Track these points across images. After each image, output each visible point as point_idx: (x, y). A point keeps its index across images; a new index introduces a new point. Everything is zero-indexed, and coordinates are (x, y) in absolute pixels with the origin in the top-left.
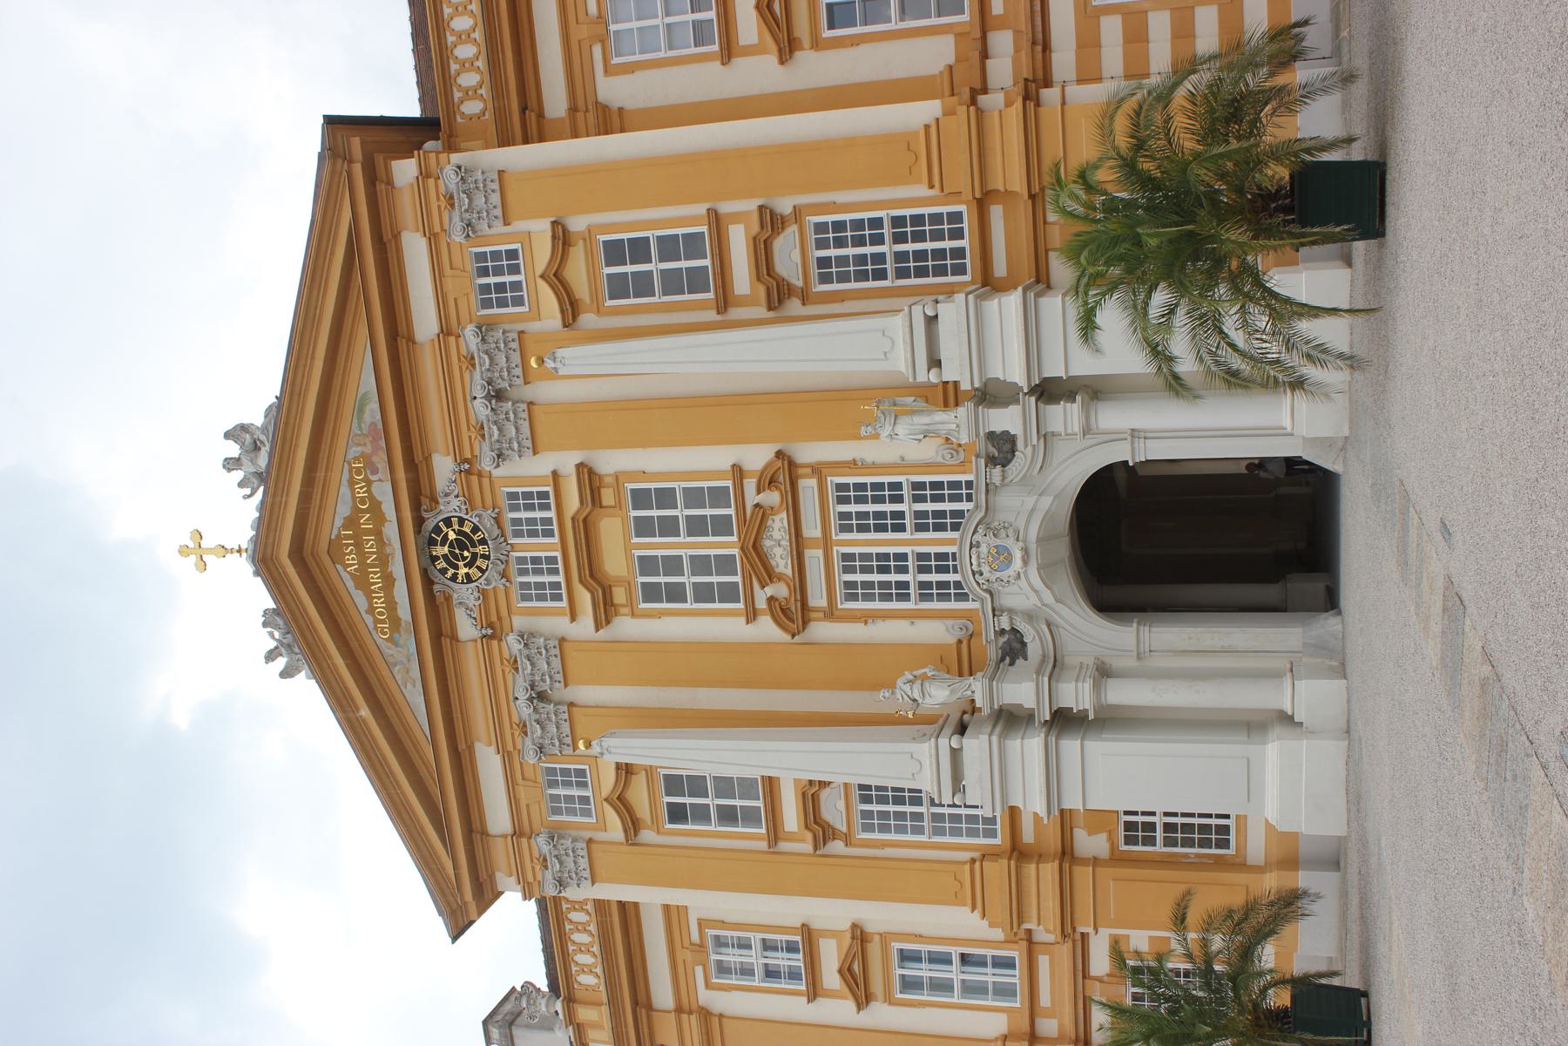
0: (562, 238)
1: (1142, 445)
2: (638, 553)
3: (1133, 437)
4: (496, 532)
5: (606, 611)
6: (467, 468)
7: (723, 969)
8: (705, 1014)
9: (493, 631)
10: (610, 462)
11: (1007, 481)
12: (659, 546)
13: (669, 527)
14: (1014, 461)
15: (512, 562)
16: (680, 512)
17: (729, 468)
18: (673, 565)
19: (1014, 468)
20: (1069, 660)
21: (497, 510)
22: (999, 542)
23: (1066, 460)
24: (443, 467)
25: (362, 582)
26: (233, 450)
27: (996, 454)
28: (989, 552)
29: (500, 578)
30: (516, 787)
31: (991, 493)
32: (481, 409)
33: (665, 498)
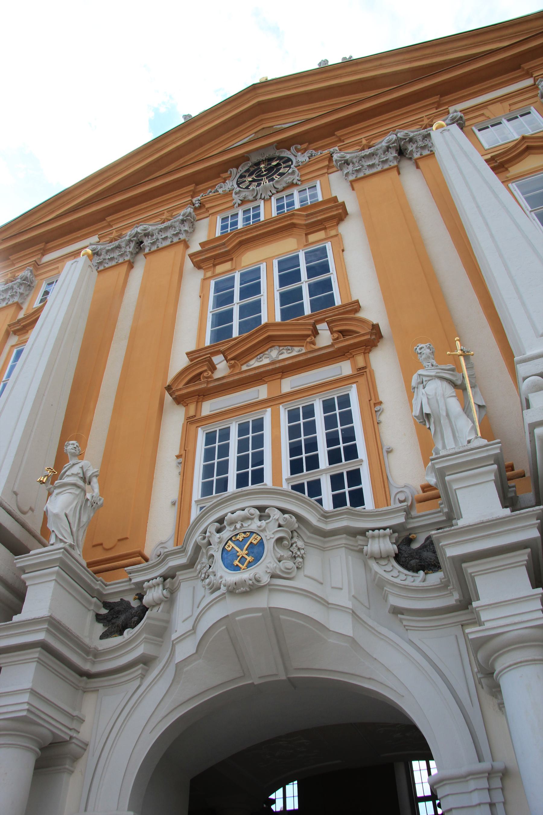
1: (476, 798)
2: (263, 267)
3: (490, 774)
4: (280, 187)
11: (373, 565)
14: (410, 573)
15: (255, 204)
17: (354, 299)
19: (395, 573)
20: (90, 701)
21: (299, 183)
22: (269, 546)
23: (419, 649)
27: (415, 546)
28: (252, 533)
29: (241, 198)
30: (74, 257)
31: (351, 541)
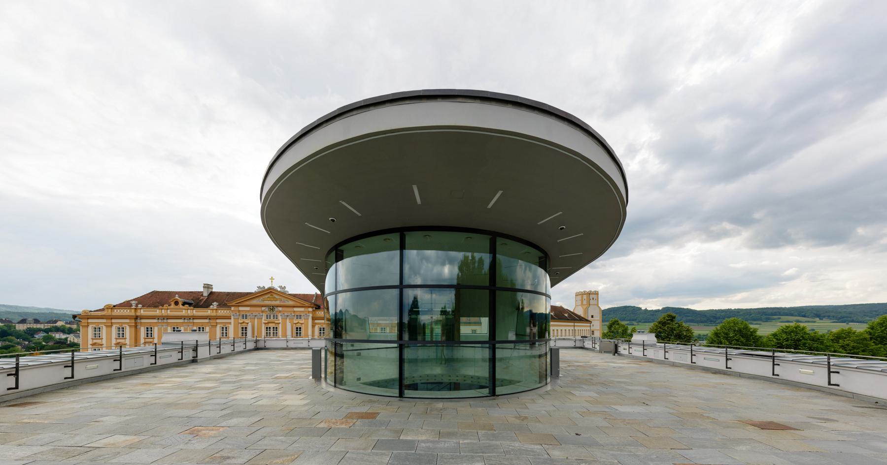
0: (302, 324)
5: (265, 323)
6: (280, 312)
7: (223, 328)
8: (216, 326)
9: (262, 312)
10: (280, 325)
12: (272, 329)
13: (274, 330)
16: (275, 332)
18: (270, 330)
24: (280, 309)
25: (269, 297)
26: (283, 286)
32: (286, 314)
33: (276, 330)
